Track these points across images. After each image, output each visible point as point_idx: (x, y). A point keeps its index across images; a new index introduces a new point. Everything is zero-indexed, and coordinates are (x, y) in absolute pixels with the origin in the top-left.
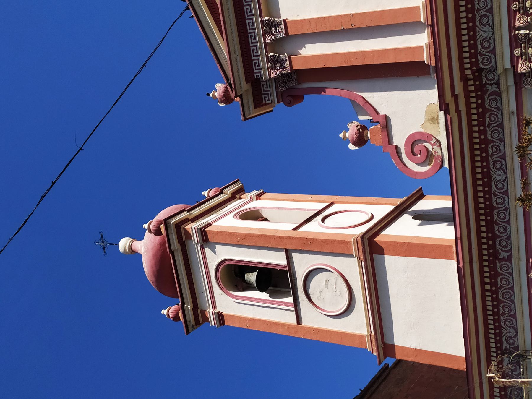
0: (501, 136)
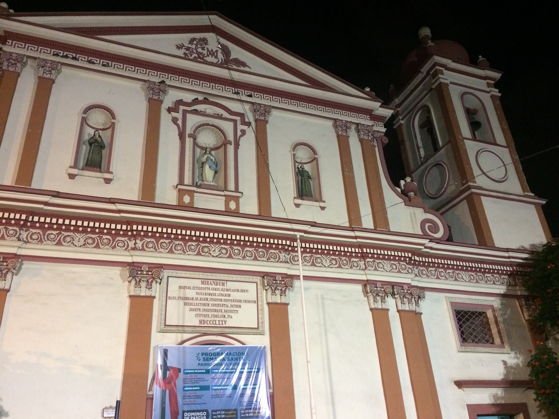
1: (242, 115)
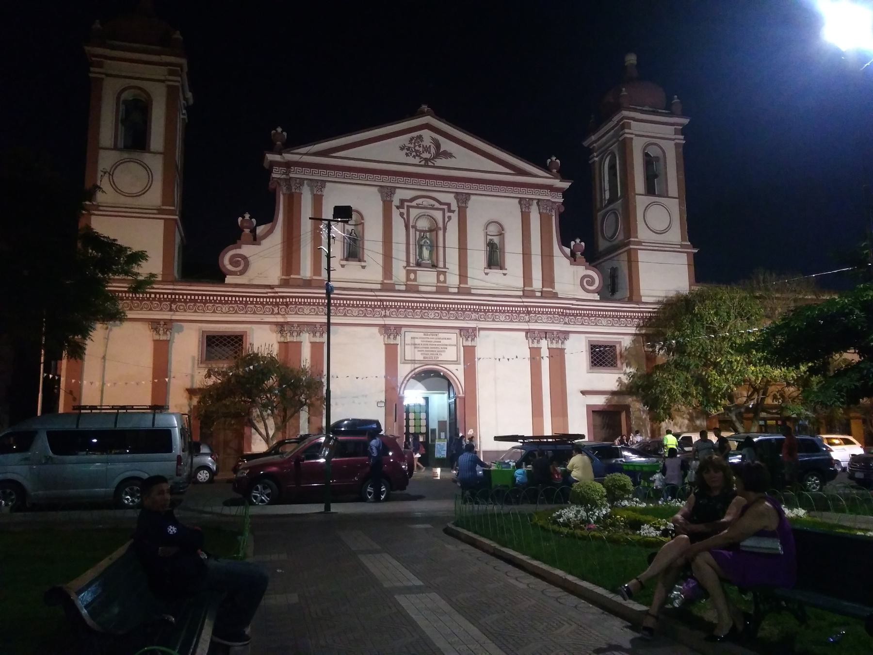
0: (249, 312)
1: (449, 205)
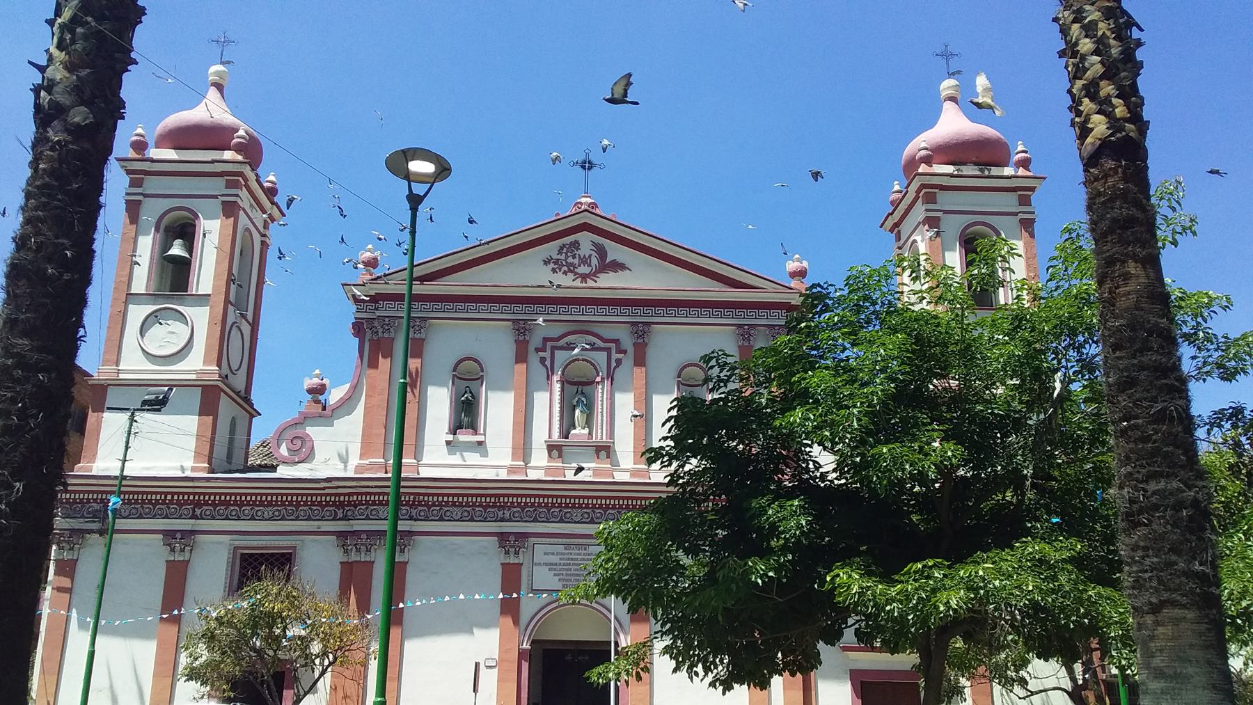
1: (616, 341)
